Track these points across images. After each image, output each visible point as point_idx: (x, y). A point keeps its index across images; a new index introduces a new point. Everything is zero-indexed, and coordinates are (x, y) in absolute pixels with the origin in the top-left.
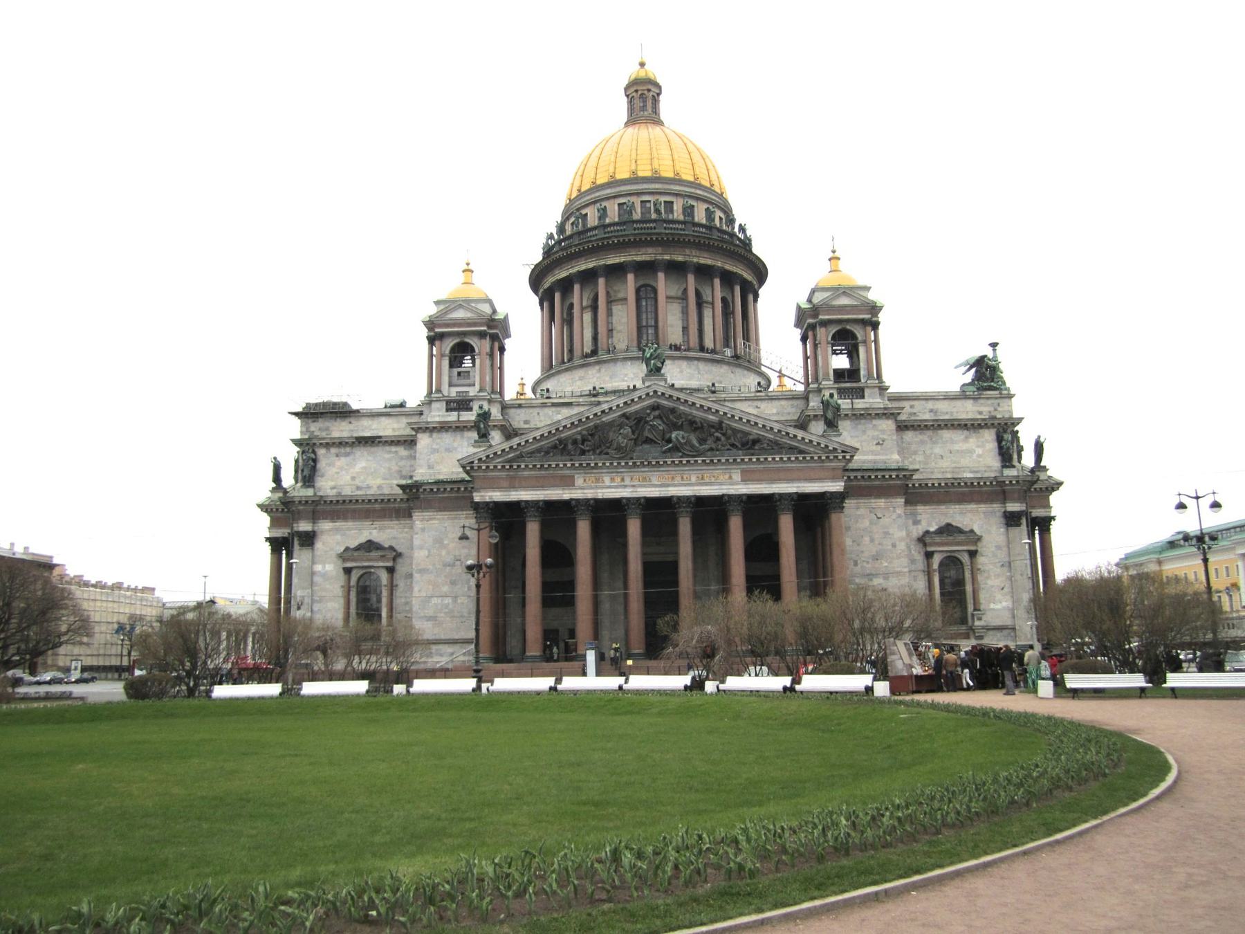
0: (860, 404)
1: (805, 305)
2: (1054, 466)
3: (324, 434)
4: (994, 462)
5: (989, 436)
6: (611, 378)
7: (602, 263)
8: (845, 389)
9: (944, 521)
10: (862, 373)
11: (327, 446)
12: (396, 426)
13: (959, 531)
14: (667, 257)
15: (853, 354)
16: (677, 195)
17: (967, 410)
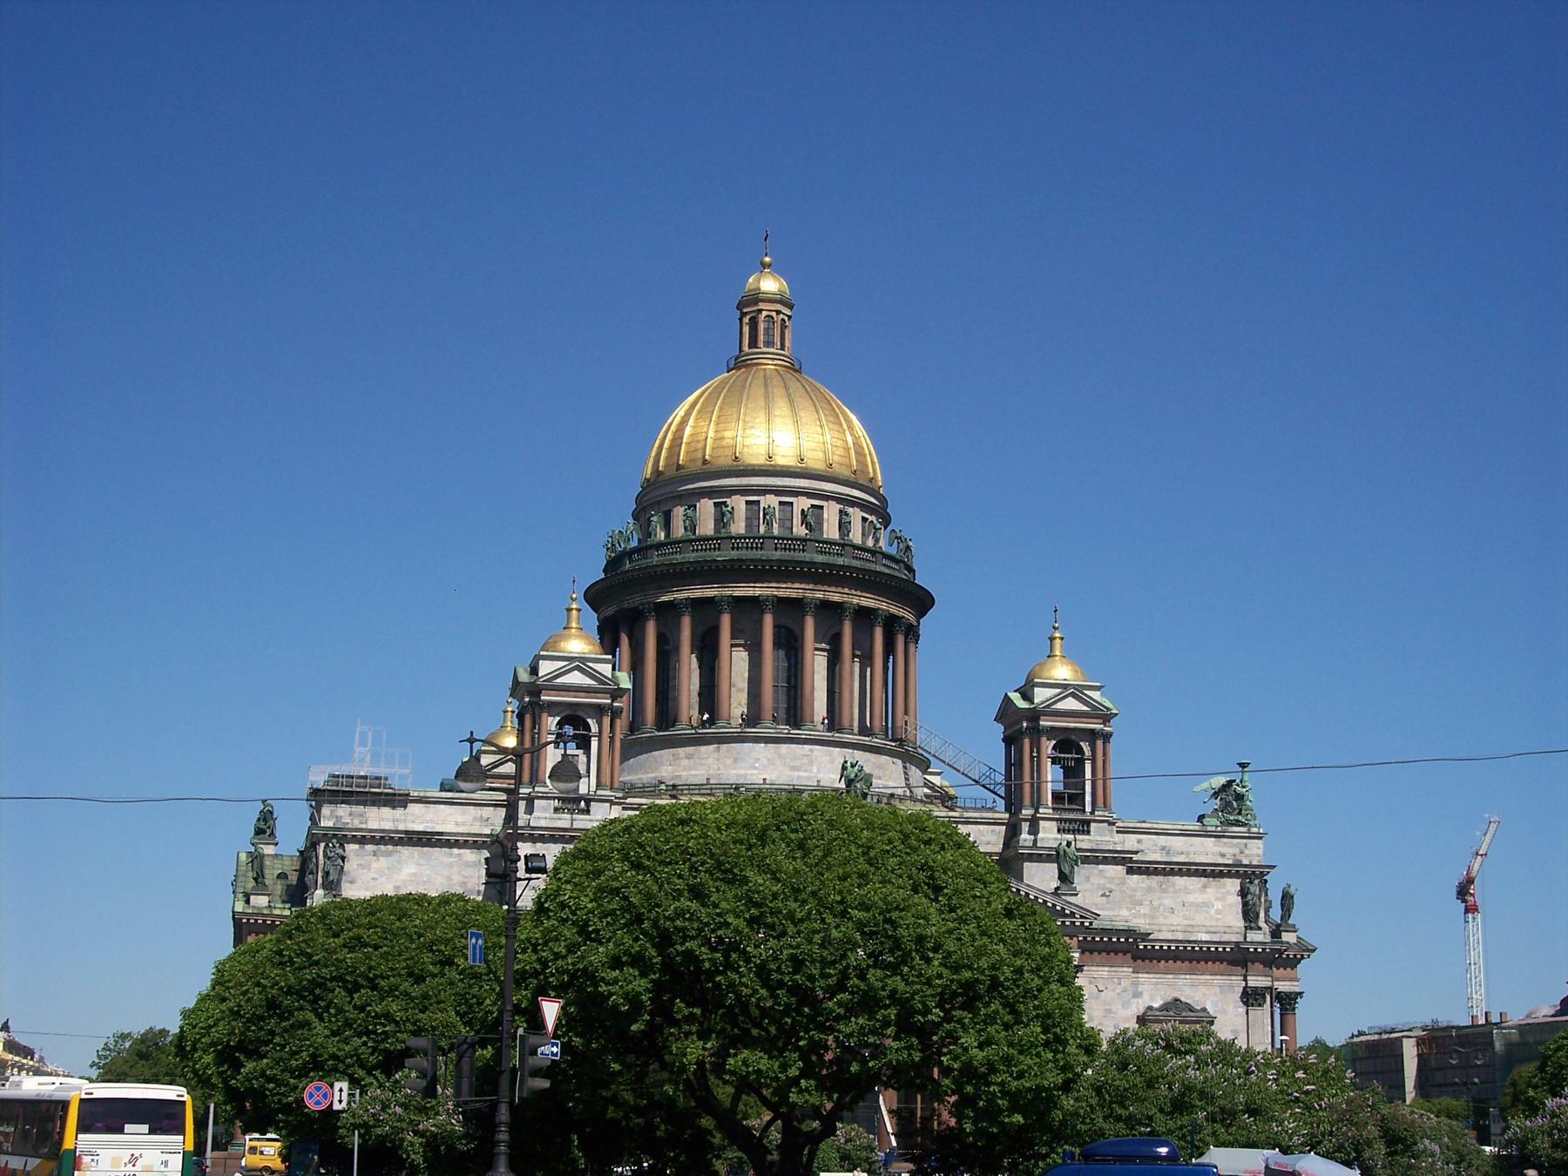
0: (1084, 842)
1: (1022, 704)
2: (1305, 925)
3: (356, 823)
4: (1241, 923)
5: (1233, 885)
6: (735, 760)
7: (727, 592)
8: (1066, 820)
9: (1170, 995)
10: (1088, 798)
11: (362, 841)
12: (460, 818)
13: (1191, 1009)
14: (819, 595)
15: (1073, 772)
16: (827, 498)
17: (1207, 850)
